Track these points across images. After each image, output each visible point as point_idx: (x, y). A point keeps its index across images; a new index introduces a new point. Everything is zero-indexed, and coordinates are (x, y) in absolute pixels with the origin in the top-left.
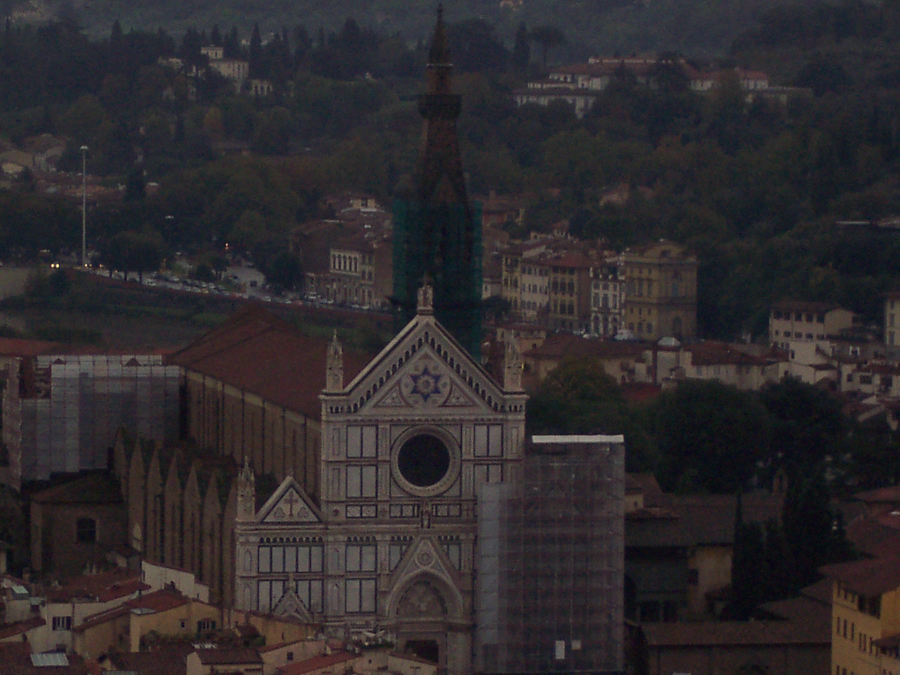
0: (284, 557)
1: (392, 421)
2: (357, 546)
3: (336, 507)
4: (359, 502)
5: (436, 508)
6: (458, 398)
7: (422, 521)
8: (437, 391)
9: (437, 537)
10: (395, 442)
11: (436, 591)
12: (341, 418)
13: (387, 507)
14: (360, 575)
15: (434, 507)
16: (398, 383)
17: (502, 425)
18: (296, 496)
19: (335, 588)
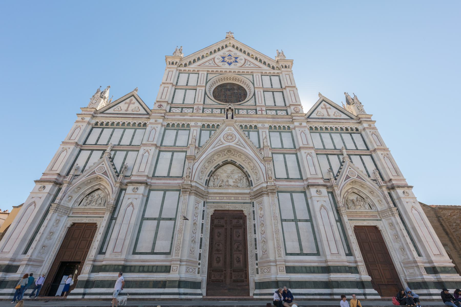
0: (111, 135)
1: (208, 71)
2: (175, 129)
3: (162, 104)
4: (181, 105)
5: (238, 111)
6: (249, 65)
7: (227, 115)
8: (236, 62)
9: (239, 125)
10: (209, 80)
11: (240, 168)
12: (176, 66)
13: (201, 107)
14: (173, 150)
15: (237, 110)
16: (214, 59)
17: (279, 76)
18: (134, 100)
19: (147, 154)
